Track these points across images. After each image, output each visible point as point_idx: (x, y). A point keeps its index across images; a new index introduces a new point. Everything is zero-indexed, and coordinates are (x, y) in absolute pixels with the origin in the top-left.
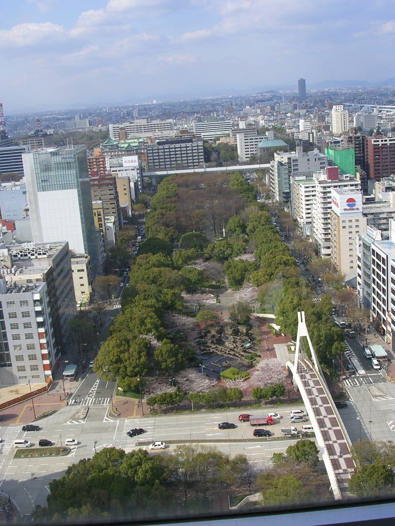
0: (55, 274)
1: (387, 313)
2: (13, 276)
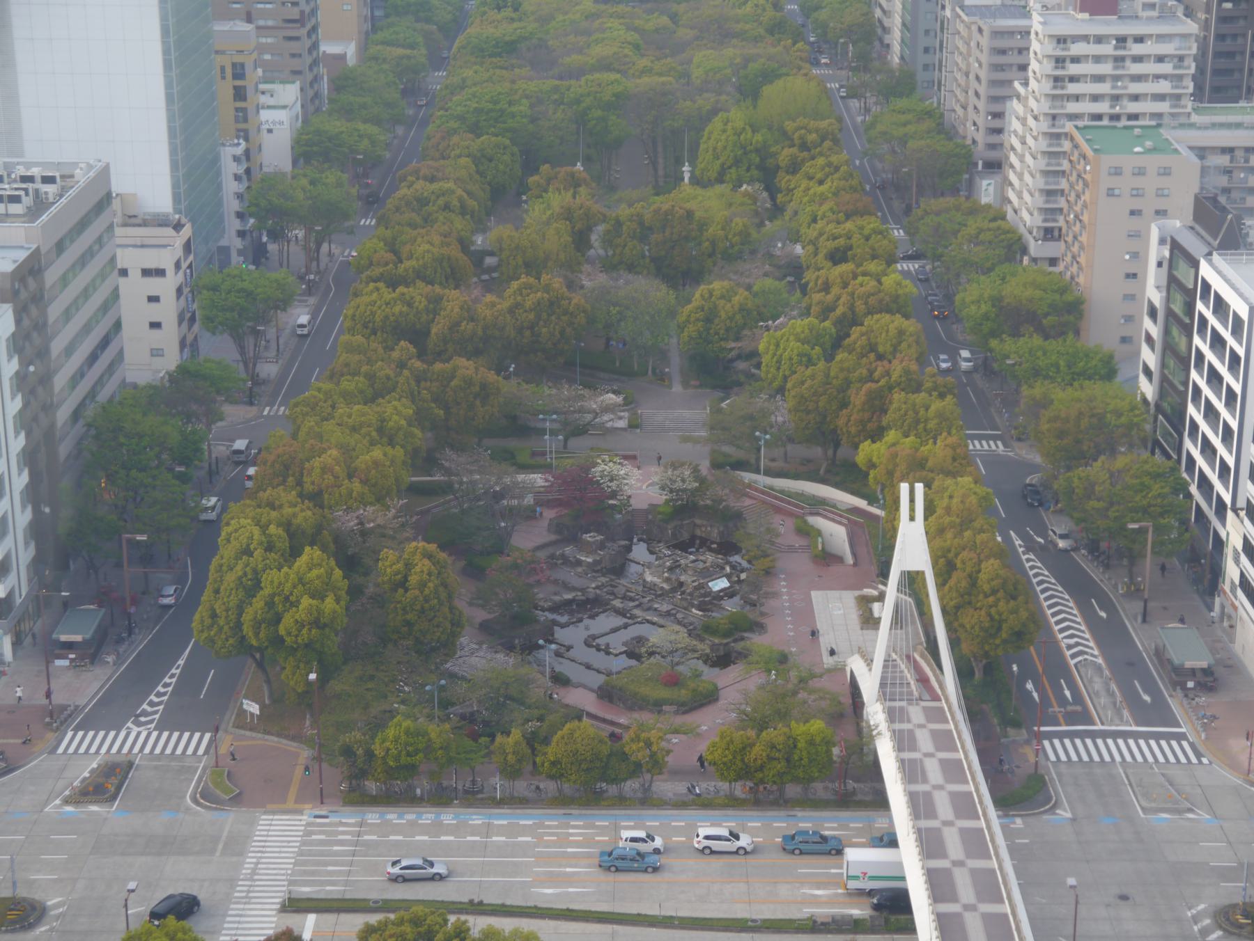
0: (51, 276)
1: (1230, 514)
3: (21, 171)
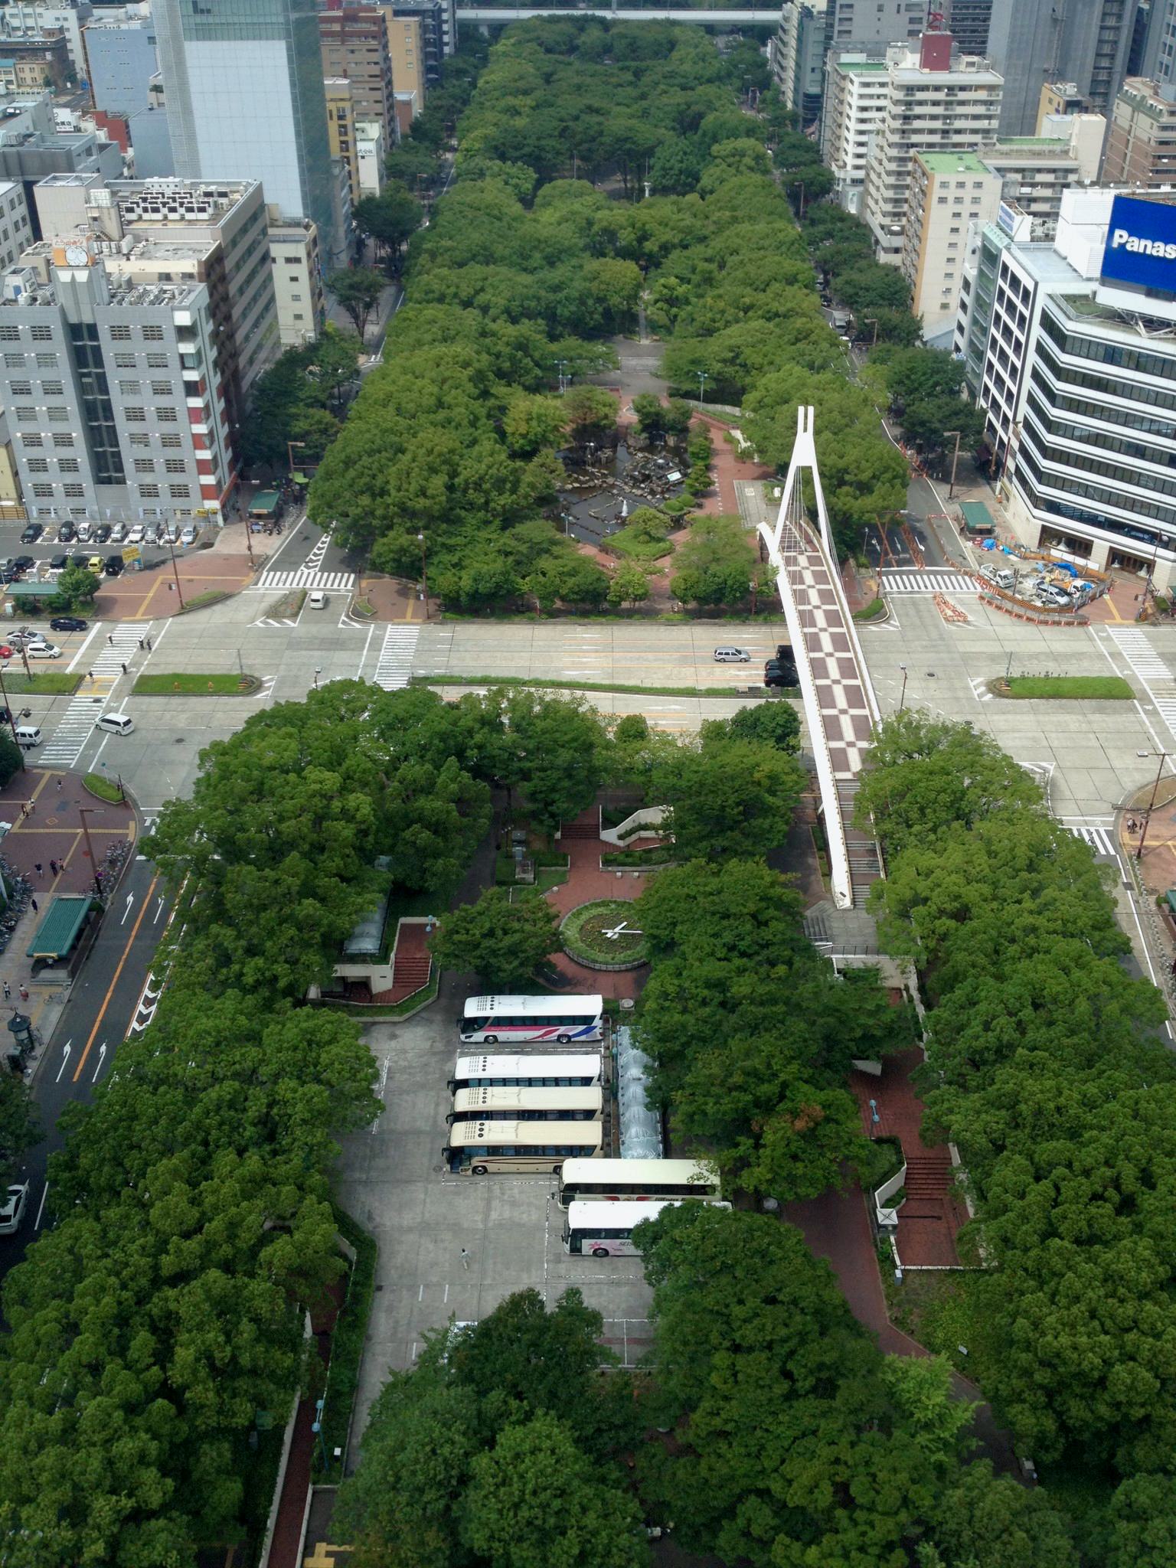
0: (229, 264)
1: (1011, 426)
2: (123, 262)
3: (203, 188)
